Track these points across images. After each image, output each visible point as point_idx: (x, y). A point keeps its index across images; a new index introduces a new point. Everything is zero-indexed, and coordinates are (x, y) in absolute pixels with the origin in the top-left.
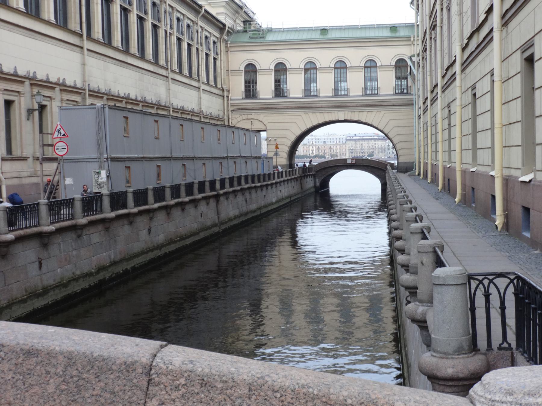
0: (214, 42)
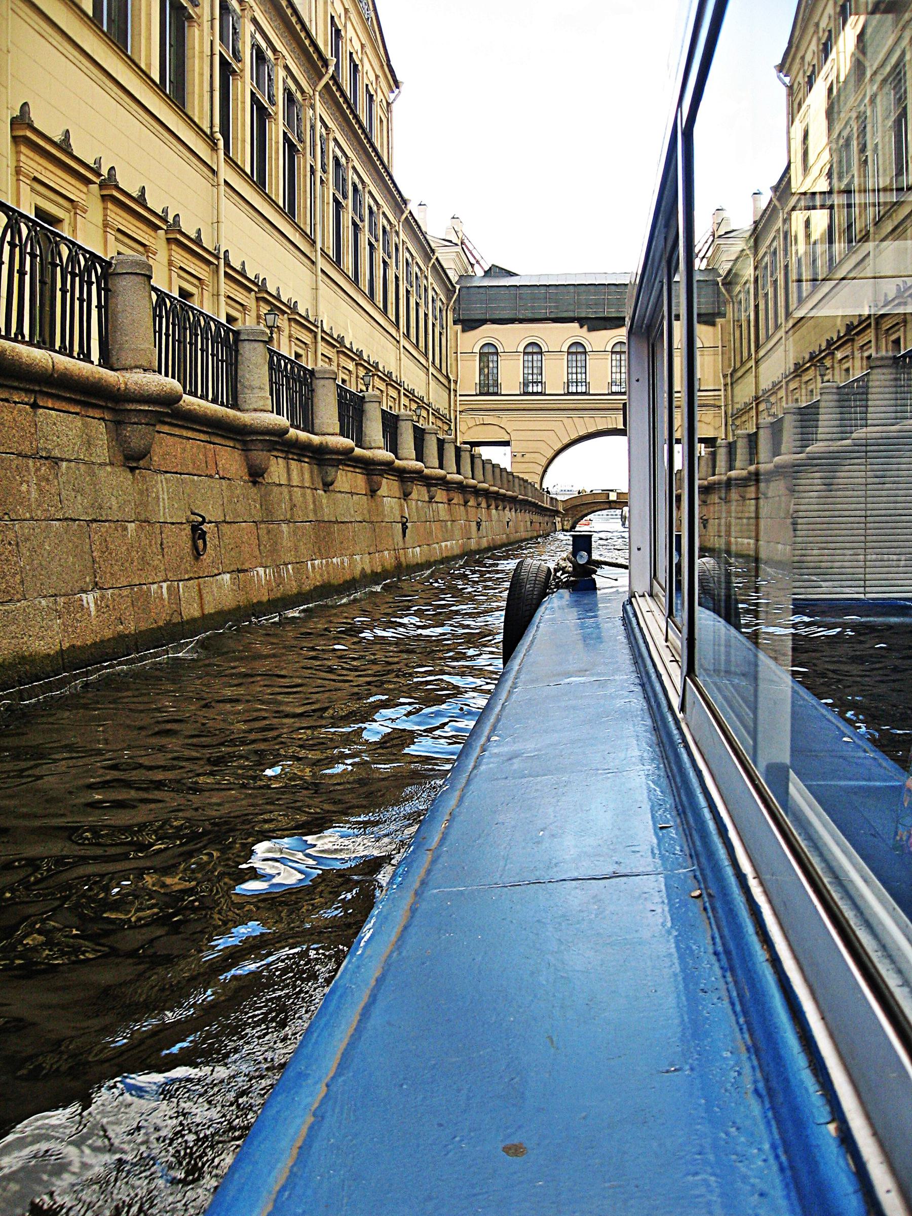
0: (441, 310)
